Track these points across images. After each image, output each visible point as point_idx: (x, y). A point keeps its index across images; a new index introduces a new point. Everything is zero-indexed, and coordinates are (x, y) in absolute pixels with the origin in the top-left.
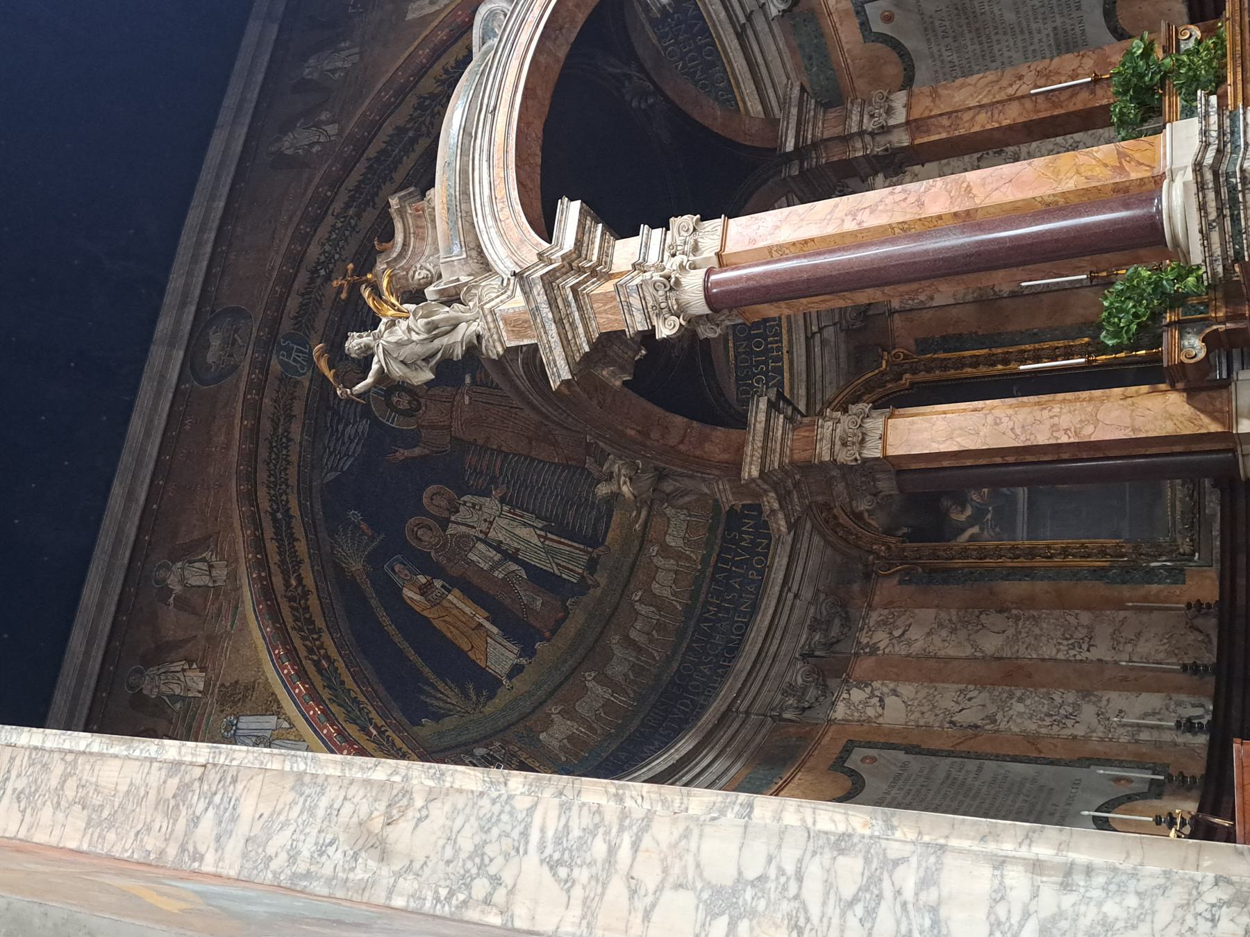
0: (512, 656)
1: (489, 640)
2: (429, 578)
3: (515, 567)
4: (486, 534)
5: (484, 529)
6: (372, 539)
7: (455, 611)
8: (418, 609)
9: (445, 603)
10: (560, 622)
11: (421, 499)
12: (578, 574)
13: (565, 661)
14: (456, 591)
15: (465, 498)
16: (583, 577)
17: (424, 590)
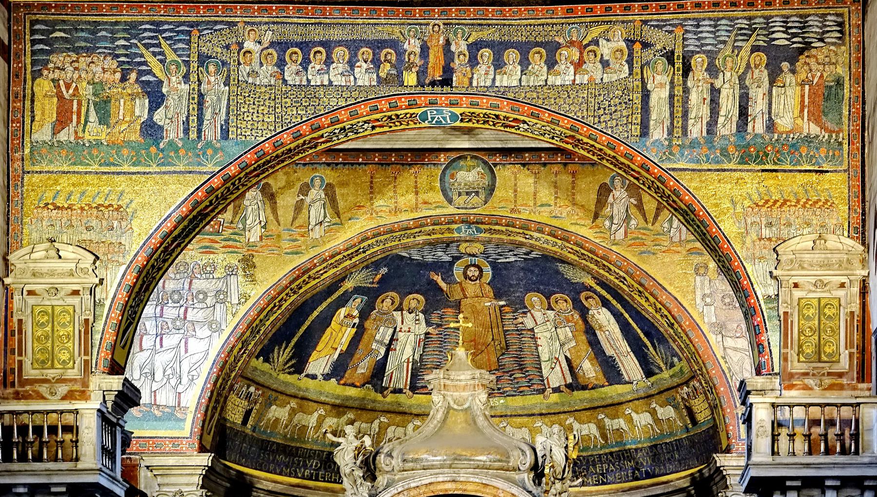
0: (321, 371)
1: (328, 357)
2: (358, 315)
3: (383, 351)
4: (400, 331)
5: (403, 330)
6: (373, 283)
7: (340, 335)
8: (334, 319)
9: (344, 329)
10: (353, 385)
11: (411, 294)
12: (389, 385)
13: (327, 396)
14: (354, 330)
15: (421, 315)
16: (387, 388)
17: (349, 316)
